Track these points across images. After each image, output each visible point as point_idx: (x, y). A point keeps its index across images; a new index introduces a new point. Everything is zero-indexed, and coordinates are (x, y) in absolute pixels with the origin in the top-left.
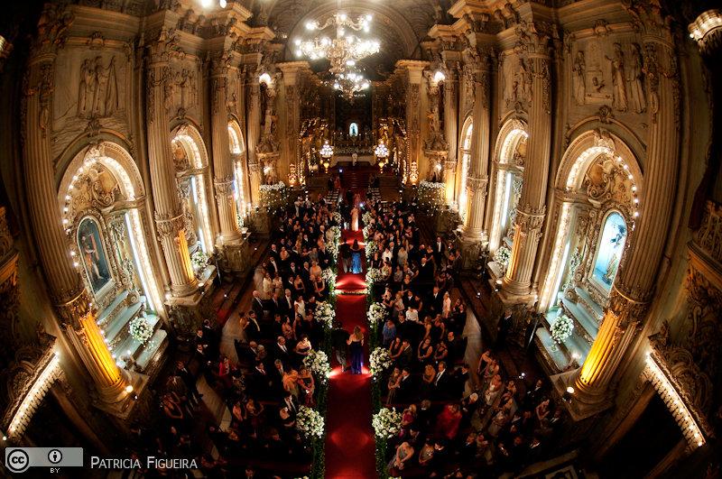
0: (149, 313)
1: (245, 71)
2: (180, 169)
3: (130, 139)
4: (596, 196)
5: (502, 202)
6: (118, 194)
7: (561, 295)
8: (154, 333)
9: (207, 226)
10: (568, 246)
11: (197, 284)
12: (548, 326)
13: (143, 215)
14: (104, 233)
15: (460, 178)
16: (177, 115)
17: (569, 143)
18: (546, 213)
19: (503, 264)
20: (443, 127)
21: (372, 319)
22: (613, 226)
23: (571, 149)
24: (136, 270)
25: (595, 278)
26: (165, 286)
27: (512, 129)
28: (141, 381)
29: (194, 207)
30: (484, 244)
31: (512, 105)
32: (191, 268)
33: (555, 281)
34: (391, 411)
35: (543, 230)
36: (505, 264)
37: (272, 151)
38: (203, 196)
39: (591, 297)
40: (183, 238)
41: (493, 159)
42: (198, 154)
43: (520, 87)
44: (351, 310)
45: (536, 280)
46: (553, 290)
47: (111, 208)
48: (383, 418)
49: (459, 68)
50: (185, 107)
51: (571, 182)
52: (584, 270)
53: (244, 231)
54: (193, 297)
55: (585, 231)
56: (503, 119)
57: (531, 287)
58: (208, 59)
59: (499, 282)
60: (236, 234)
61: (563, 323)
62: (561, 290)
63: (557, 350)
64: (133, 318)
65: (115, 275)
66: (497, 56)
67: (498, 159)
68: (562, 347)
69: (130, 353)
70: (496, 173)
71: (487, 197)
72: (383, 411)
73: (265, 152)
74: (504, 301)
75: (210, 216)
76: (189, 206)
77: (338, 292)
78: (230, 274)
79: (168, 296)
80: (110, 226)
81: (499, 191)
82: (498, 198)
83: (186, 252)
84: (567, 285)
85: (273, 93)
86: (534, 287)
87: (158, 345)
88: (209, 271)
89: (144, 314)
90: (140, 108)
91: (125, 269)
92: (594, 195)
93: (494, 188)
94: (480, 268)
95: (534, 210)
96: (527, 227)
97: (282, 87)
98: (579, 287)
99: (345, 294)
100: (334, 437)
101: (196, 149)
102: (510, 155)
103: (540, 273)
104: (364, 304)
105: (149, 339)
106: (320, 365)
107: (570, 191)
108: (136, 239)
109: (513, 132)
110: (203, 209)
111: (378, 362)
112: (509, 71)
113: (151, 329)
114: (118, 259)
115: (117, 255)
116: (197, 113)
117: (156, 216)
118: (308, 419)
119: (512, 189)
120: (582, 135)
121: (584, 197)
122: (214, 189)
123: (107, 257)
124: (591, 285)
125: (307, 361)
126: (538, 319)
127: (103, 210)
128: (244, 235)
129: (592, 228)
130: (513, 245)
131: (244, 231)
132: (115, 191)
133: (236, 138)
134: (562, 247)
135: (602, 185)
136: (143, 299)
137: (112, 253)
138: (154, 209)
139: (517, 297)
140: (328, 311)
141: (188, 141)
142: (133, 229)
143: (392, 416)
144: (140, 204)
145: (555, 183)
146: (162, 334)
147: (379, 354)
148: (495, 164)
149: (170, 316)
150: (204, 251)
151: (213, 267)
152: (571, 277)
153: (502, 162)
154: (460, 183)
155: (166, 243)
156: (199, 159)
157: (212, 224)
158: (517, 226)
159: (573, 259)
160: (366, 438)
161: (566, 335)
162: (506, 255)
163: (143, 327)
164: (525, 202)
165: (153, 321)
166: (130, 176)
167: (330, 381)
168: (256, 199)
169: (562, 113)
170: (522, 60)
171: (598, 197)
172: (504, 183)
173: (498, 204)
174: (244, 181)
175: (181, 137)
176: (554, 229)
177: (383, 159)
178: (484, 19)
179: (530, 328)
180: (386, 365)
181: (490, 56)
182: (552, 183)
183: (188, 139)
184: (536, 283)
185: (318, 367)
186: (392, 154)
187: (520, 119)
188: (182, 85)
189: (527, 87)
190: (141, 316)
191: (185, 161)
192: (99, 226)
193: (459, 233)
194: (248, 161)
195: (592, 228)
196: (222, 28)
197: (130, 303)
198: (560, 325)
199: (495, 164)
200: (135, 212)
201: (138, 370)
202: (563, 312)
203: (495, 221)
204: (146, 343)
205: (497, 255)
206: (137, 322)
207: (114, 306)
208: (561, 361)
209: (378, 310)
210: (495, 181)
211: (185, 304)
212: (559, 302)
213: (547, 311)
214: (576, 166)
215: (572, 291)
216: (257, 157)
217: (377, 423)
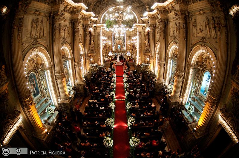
0: (52, 105)
1: (84, 26)
2: (63, 58)
3: (47, 46)
4: (201, 66)
6: (43, 65)
7: (190, 99)
8: (54, 112)
9: (72, 77)
10: (192, 83)
11: (69, 96)
12: (186, 109)
13: (51, 72)
14: (38, 78)
16: (63, 40)
17: (192, 49)
18: (185, 72)
19: (171, 89)
20: (149, 46)
21: (128, 108)
22: (206, 76)
23: (193, 51)
24: (48, 91)
25: (200, 93)
26: (58, 96)
27: (173, 45)
28: (50, 128)
29: (68, 71)
30: (164, 84)
31: (173, 38)
32: (67, 91)
33: (188, 94)
34: (136, 138)
35: (184, 78)
36: (171, 89)
37: (93, 53)
38: (71, 67)
39: (199, 99)
40: (64, 80)
41: (166, 56)
42: (69, 53)
43: (175, 32)
44: (121, 105)
45: (181, 94)
46: (187, 97)
47: (40, 69)
48: (133, 140)
49: (154, 26)
50: (66, 37)
51: (193, 62)
52: (197, 90)
53: (84, 79)
54: (68, 100)
55: (197, 78)
56: (170, 42)
57: (180, 97)
58: (73, 21)
59: (170, 95)
60: (81, 80)
61: (191, 108)
62: (190, 97)
63: (189, 117)
64: (47, 107)
65: (41, 92)
67: (168, 56)
68: (191, 116)
69: (46, 118)
70: (167, 60)
71: (164, 68)
72: (133, 138)
73: (91, 53)
74: (171, 101)
75: (73, 74)
77: (116, 99)
78: (80, 92)
79: (59, 100)
80: (40, 76)
81: (168, 66)
82: (168, 68)
83: (66, 85)
84: (192, 96)
85: (93, 34)
86: (181, 96)
87: (56, 116)
88: (72, 93)
89: (51, 106)
90: (51, 36)
91: (45, 91)
92: (200, 66)
93: (167, 65)
94: (162, 91)
95: (181, 71)
96: (179, 77)
97: (96, 32)
98: (195, 96)
99: (118, 100)
100: (116, 147)
101: (69, 51)
102: (172, 54)
103: (183, 92)
104: (125, 104)
105: (53, 114)
106: (111, 123)
107: (193, 65)
108: (49, 80)
109: (173, 47)
110: (71, 71)
111: (131, 122)
112: (172, 26)
113: (53, 111)
114: (42, 87)
115: (42, 86)
116: (69, 39)
117: (56, 73)
118: (108, 141)
119: (173, 65)
120: (196, 47)
121: (197, 67)
122: (74, 65)
123: (39, 86)
124: (200, 95)
125: (107, 122)
126: (182, 107)
127: (38, 70)
128: (84, 81)
129: (200, 76)
130: (174, 84)
131: (84, 79)
132: (42, 64)
133: (81, 49)
134: (190, 83)
135: (203, 63)
136: (51, 101)
137: (40, 85)
138: (55, 70)
139: (176, 100)
140: (113, 106)
141: (66, 49)
142: (48, 77)
143: (136, 140)
144: (50, 68)
145: (188, 63)
146: (57, 113)
147: (131, 119)
148: (167, 57)
149: (60, 107)
150: (71, 86)
151: (74, 91)
152: (193, 93)
153: (169, 56)
154: (155, 64)
155: (59, 82)
156: (70, 55)
157: (73, 77)
158: (176, 77)
159: (193, 87)
160: (127, 147)
161: (192, 112)
162: (171, 87)
163: (51, 110)
164: (178, 68)
165: (54, 108)
166: (47, 59)
167: (114, 128)
168: (88, 69)
169: (189, 40)
170: (176, 23)
171: (201, 67)
172: (170, 63)
173: (168, 70)
174: (84, 63)
175: (64, 47)
176: (188, 77)
177: (129, 57)
178: (163, 9)
179: (180, 110)
180: (133, 123)
181: (165, 22)
182: (187, 62)
183: (66, 48)
184: (182, 95)
185: (111, 124)
186: (132, 55)
187: (175, 42)
188: (65, 30)
189: (178, 32)
190: (50, 106)
191: (65, 55)
192: (36, 75)
193: (155, 80)
195: (200, 76)
196: (77, 11)
197: (46, 102)
198: (190, 108)
199: (167, 57)
200: (49, 71)
201: (49, 124)
202: (190, 105)
203: (167, 76)
204: (52, 115)
205: (168, 87)
206: (48, 108)
207: (41, 102)
208: (191, 120)
209: (130, 105)
210: (167, 63)
211: (65, 103)
212: (189, 101)
213: (185, 104)
214: (194, 57)
215: (193, 98)
217: (131, 142)
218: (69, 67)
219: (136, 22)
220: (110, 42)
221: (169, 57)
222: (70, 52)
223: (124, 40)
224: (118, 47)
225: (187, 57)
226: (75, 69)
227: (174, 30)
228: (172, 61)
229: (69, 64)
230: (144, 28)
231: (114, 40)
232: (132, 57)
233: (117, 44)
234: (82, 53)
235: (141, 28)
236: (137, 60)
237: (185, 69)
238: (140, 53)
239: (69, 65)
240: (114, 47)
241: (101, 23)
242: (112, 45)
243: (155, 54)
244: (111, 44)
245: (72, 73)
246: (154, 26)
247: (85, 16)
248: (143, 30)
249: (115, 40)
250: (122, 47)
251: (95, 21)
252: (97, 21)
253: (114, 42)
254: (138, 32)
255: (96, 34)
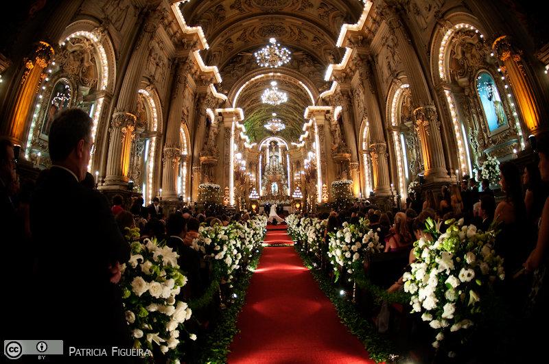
1: (197, 97)
5: (402, 157)
15: (364, 175)
35: (439, 119)
38: (153, 154)
49: (350, 94)
66: (373, 60)
71: (388, 158)
76: (139, 163)
82: (398, 154)
97: (222, 129)
101: (155, 115)
119: (406, 146)
133: (185, 141)
153: (393, 125)
154: (364, 179)
156: (156, 125)
168: (196, 196)
172: (400, 141)
174: (187, 178)
177: (299, 201)
182: (431, 83)
194: (192, 165)
203: (400, 174)
216: (199, 161)
218: (149, 155)
219: (311, 105)
220: (253, 175)
221: (394, 127)
222: (158, 118)
223: (286, 174)
224: (273, 189)
225: (428, 74)
226: (162, 163)
227: (389, 62)
228: (402, 137)
229: (150, 146)
230: (328, 115)
231: (263, 174)
232: (305, 205)
233: (270, 182)
234: (185, 153)
235: (323, 118)
236: (319, 192)
237: (433, 98)
238: (323, 174)
239: (150, 149)
240: (264, 188)
241: (234, 105)
242: (257, 183)
243: (360, 157)
244: (255, 180)
245: (151, 170)
246: (350, 94)
247: (200, 77)
248: (327, 122)
249: (266, 173)
250: (281, 187)
251: (220, 102)
252: (224, 102)
253: (262, 178)
254: (316, 127)
255: (223, 132)
